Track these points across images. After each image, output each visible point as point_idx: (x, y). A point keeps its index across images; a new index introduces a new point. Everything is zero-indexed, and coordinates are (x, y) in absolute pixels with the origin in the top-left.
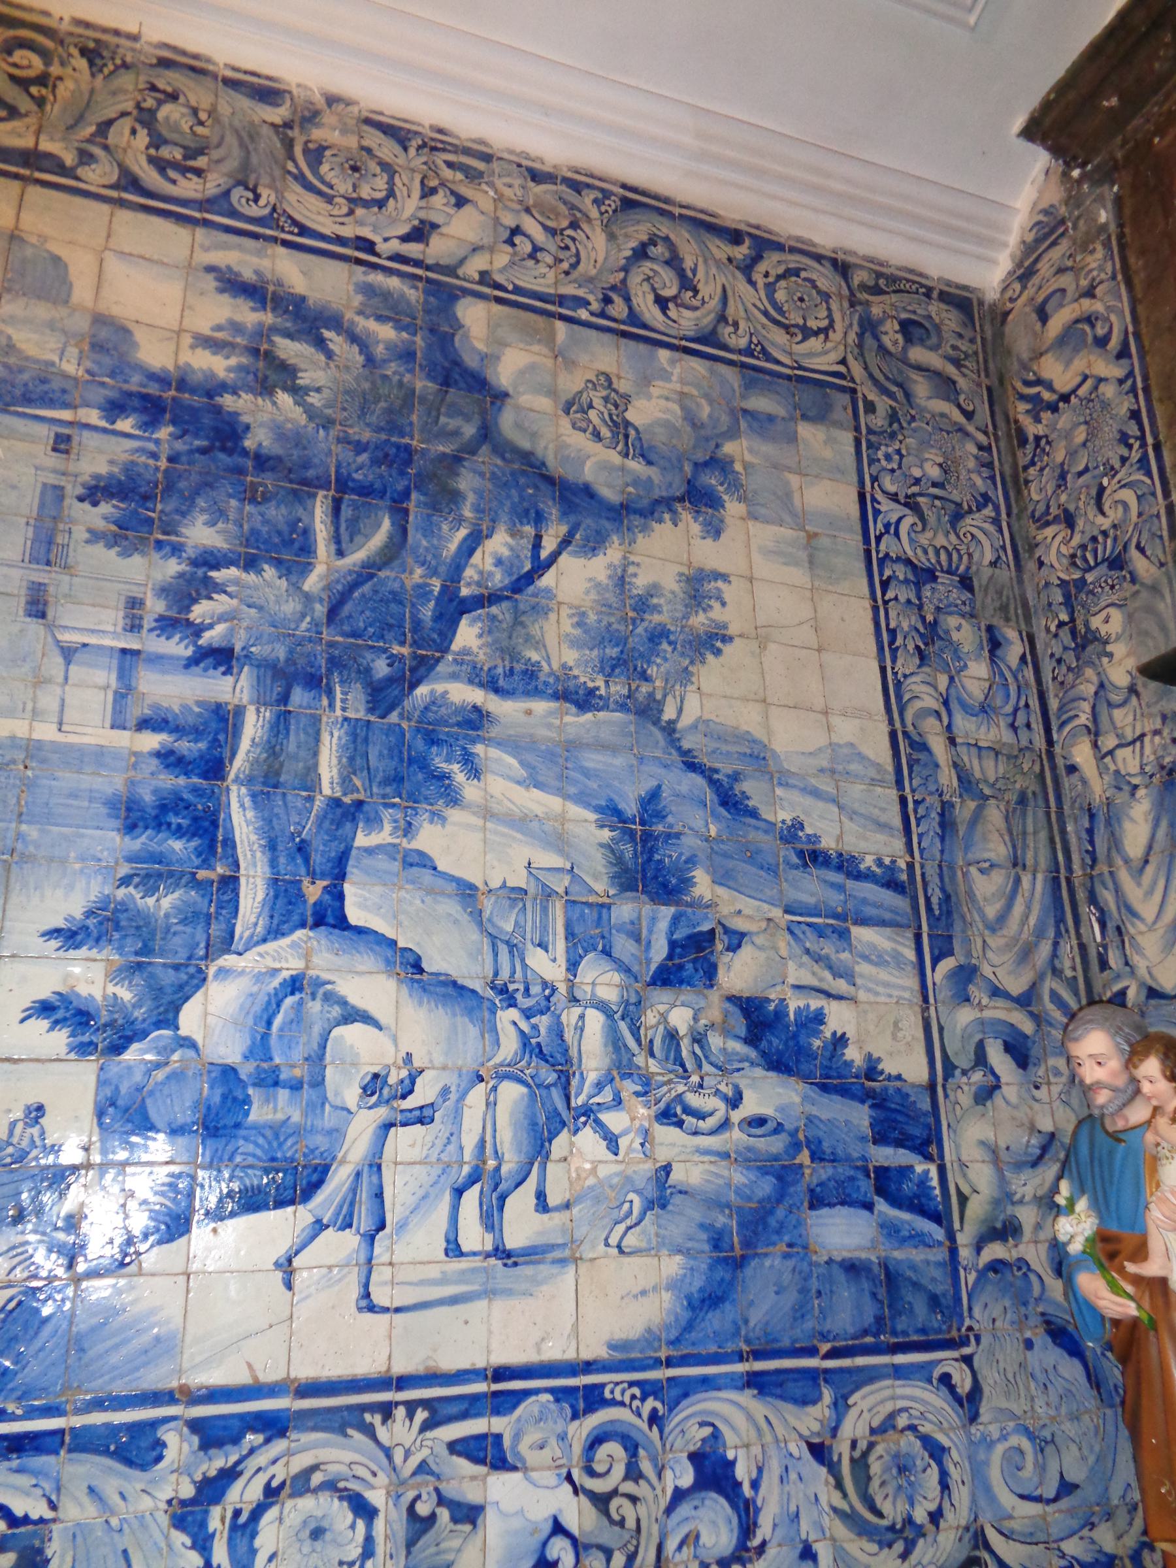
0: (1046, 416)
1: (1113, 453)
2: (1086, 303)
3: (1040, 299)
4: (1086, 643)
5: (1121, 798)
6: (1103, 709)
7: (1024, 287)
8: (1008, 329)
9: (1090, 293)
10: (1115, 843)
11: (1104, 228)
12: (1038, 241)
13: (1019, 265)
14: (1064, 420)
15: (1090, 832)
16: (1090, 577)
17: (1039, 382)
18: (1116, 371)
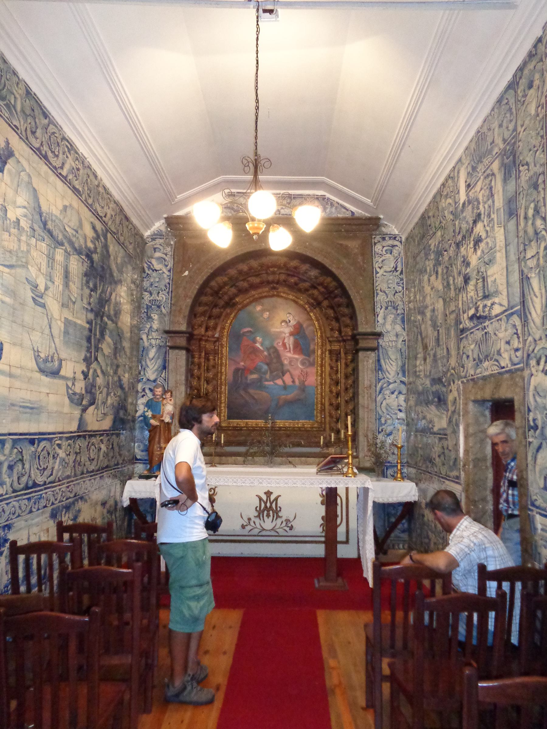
0: (151, 271)
1: (164, 288)
2: (164, 256)
3: (155, 246)
4: (149, 318)
5: (150, 347)
6: (150, 332)
7: (152, 241)
8: (146, 247)
9: (166, 255)
10: (147, 354)
11: (172, 245)
12: (157, 235)
13: (152, 236)
14: (154, 274)
15: (143, 351)
16: (153, 306)
17: (151, 263)
18: (168, 273)
